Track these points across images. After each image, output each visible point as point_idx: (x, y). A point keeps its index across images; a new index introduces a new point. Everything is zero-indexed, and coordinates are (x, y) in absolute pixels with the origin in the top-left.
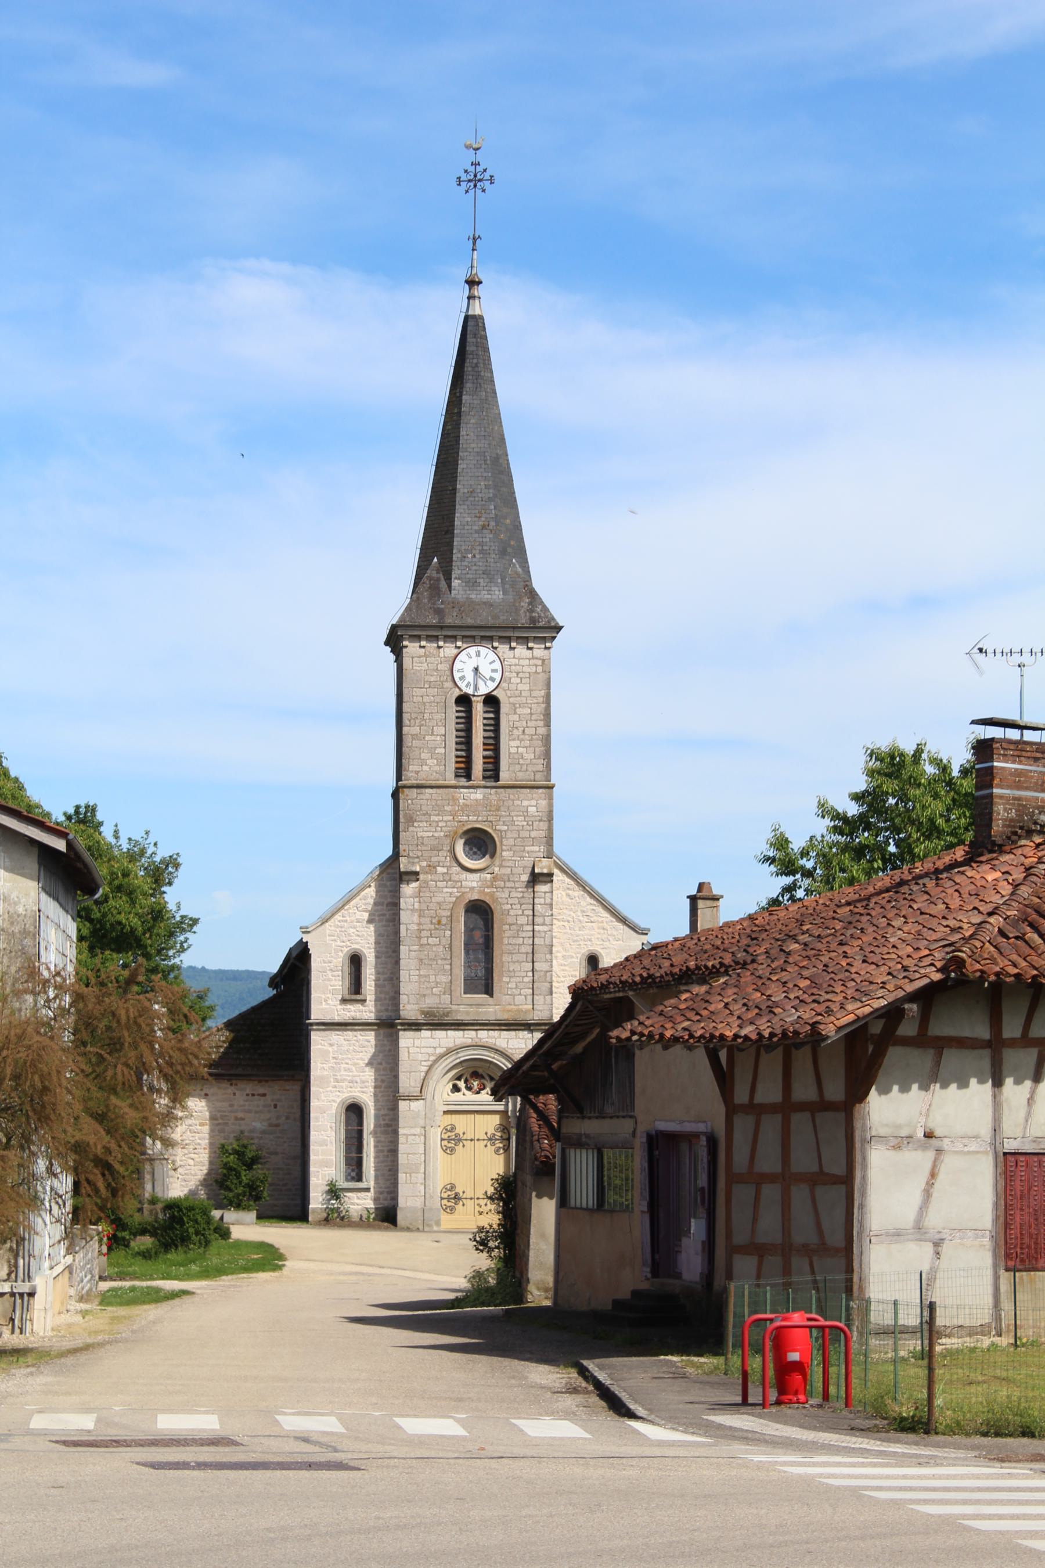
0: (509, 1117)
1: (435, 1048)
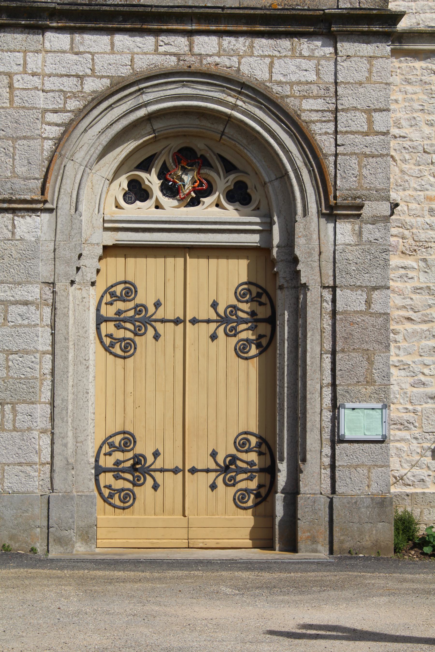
0: (273, 263)
1: (81, 78)
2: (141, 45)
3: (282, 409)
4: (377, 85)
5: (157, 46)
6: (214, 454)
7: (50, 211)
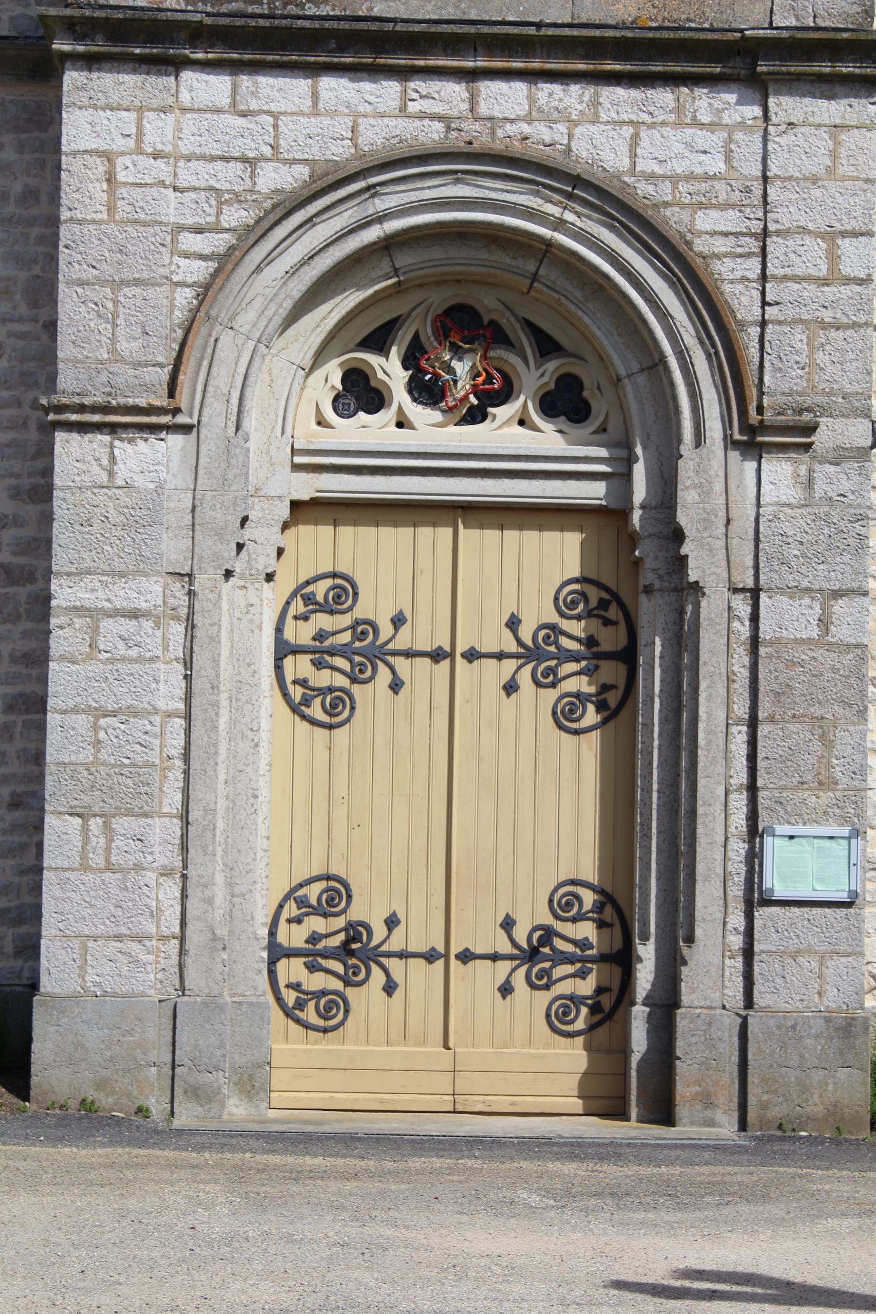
0: (633, 539)
2: (372, 99)
3: (647, 836)
4: (848, 183)
5: (405, 100)
6: (508, 924)
7: (186, 429)
